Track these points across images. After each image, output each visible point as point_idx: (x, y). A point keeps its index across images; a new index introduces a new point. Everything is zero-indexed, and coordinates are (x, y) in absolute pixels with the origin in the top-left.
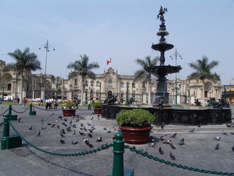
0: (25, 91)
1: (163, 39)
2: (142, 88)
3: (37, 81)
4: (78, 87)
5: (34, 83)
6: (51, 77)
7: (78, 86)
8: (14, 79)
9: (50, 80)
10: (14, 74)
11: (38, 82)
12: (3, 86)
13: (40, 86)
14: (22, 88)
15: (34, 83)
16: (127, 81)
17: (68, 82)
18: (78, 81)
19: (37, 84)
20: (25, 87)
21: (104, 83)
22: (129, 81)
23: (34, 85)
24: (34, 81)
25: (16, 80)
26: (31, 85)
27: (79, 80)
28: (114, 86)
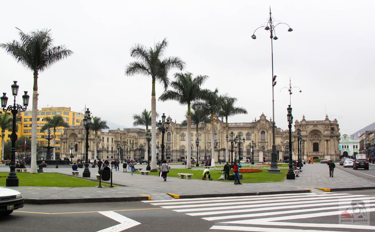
2: (260, 141)
3: (112, 139)
4: (171, 143)
7: (171, 142)
11: (114, 140)
12: (71, 147)
16: (239, 131)
18: (171, 135)
19: (113, 142)
21: (205, 135)
22: (242, 131)
23: (108, 144)
24: (107, 139)
26: (103, 144)
27: (173, 134)
28: (219, 140)
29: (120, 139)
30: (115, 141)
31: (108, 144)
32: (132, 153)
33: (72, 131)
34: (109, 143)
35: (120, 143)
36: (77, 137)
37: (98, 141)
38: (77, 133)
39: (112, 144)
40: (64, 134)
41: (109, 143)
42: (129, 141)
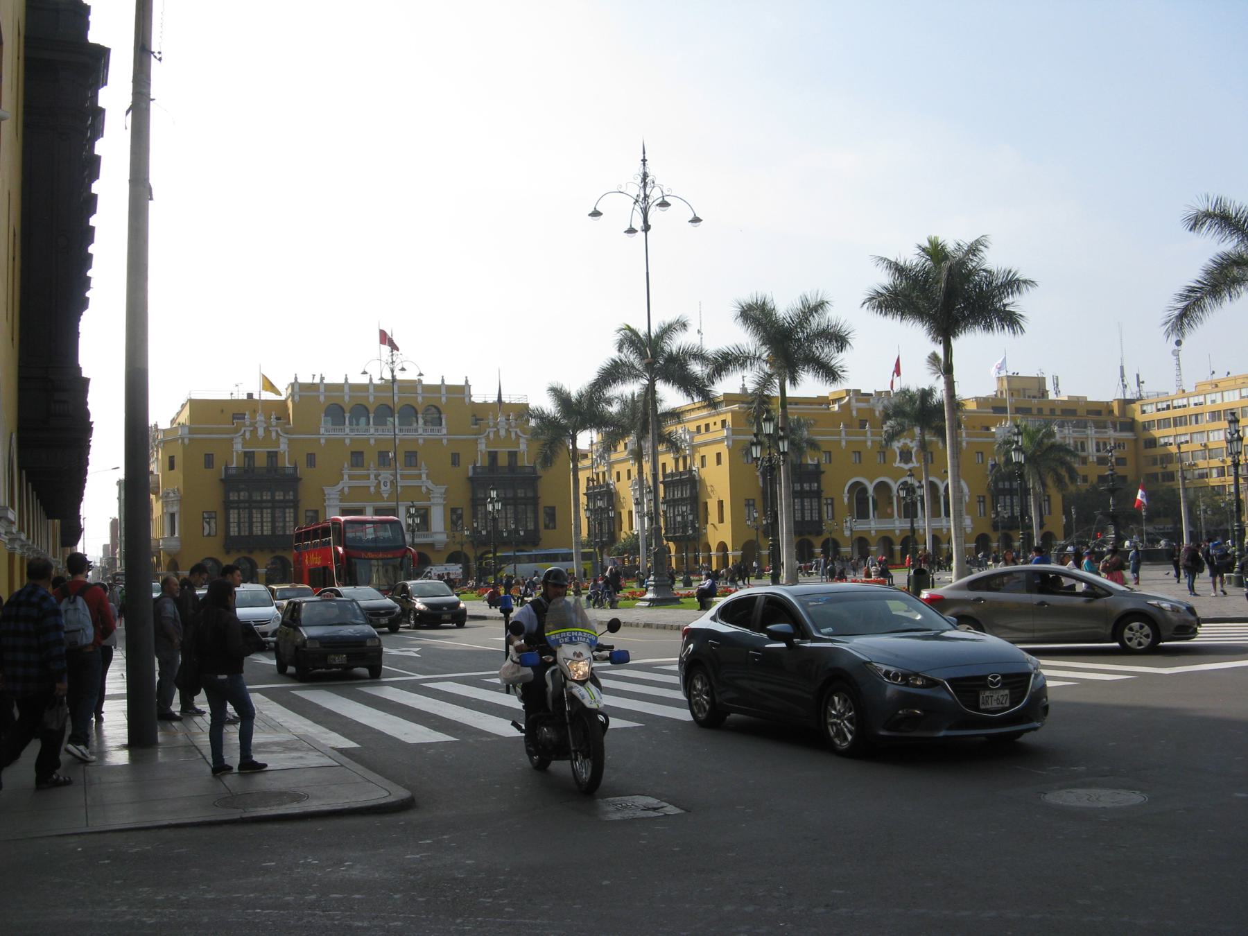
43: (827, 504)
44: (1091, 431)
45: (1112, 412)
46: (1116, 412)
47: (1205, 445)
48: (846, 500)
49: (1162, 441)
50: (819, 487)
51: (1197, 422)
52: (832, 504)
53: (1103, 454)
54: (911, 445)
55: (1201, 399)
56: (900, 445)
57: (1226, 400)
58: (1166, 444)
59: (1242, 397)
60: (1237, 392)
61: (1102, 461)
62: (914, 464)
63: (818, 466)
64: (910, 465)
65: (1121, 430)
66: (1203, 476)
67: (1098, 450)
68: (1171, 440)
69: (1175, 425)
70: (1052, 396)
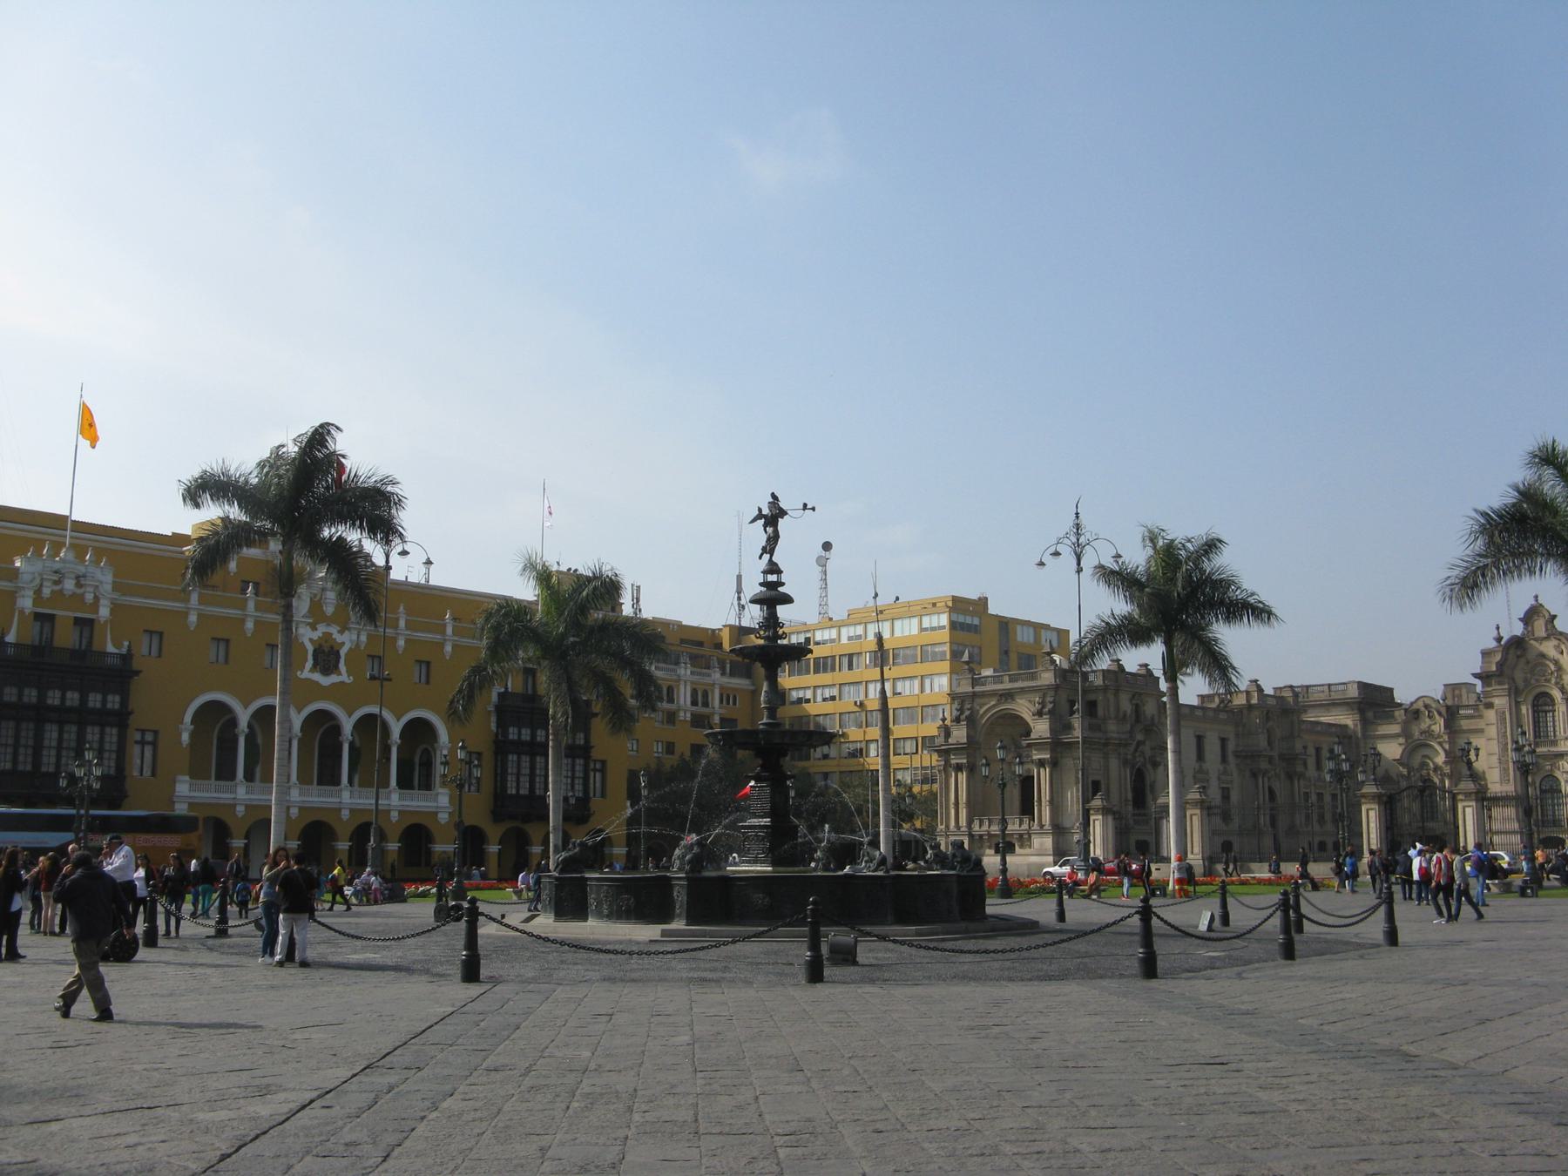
0: (1110, 818)
1: (771, 622)
3: (1223, 741)
5: (1200, 756)
6: (1353, 692)
8: (1039, 746)
9: (1348, 719)
10: (1040, 714)
11: (1231, 746)
13: (1254, 775)
14: (1086, 800)
15: (1200, 756)
17: (1480, 724)
19: (1231, 758)
20: (1114, 787)
23: (1201, 771)
24: (1193, 741)
25: (1053, 751)
29: (1263, 743)
30: (1237, 755)
31: (1201, 771)
32: (1469, 811)
33: (999, 703)
34: (1206, 766)
35: (1264, 765)
36: (1028, 732)
37: (1148, 753)
38: (1027, 717)
39: (1225, 772)
40: (957, 720)
41: (1206, 766)
42: (1311, 751)
43: (142, 743)
44: (685, 671)
45: (719, 646)
46: (726, 646)
47: (862, 705)
48: (185, 737)
49: (795, 695)
50: (124, 702)
51: (850, 667)
52: (154, 744)
53: (700, 709)
54: (339, 638)
55: (859, 630)
56: (316, 635)
57: (898, 633)
58: (800, 701)
59: (922, 630)
60: (915, 621)
61: (699, 721)
62: (343, 676)
63: (127, 658)
64: (334, 679)
65: (732, 675)
66: (859, 753)
67: (694, 703)
68: (809, 694)
69: (817, 671)
70: (627, 610)
